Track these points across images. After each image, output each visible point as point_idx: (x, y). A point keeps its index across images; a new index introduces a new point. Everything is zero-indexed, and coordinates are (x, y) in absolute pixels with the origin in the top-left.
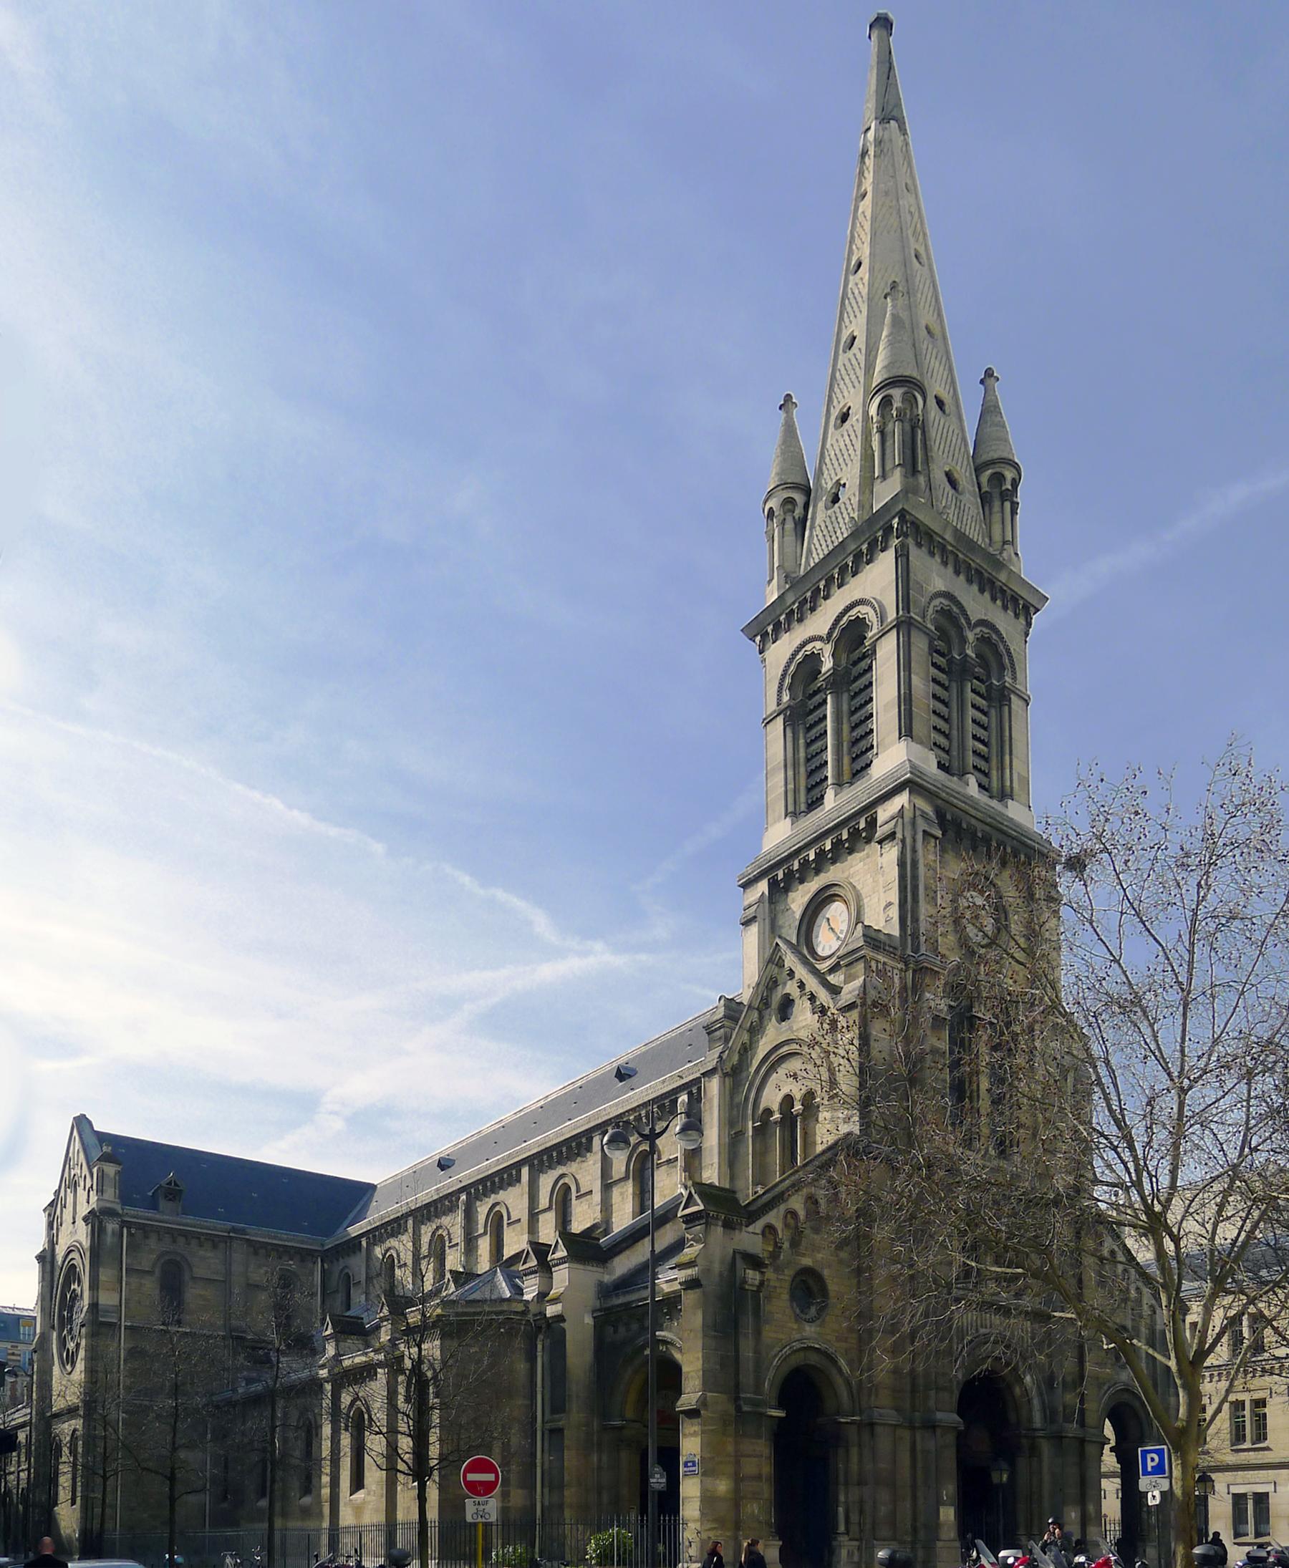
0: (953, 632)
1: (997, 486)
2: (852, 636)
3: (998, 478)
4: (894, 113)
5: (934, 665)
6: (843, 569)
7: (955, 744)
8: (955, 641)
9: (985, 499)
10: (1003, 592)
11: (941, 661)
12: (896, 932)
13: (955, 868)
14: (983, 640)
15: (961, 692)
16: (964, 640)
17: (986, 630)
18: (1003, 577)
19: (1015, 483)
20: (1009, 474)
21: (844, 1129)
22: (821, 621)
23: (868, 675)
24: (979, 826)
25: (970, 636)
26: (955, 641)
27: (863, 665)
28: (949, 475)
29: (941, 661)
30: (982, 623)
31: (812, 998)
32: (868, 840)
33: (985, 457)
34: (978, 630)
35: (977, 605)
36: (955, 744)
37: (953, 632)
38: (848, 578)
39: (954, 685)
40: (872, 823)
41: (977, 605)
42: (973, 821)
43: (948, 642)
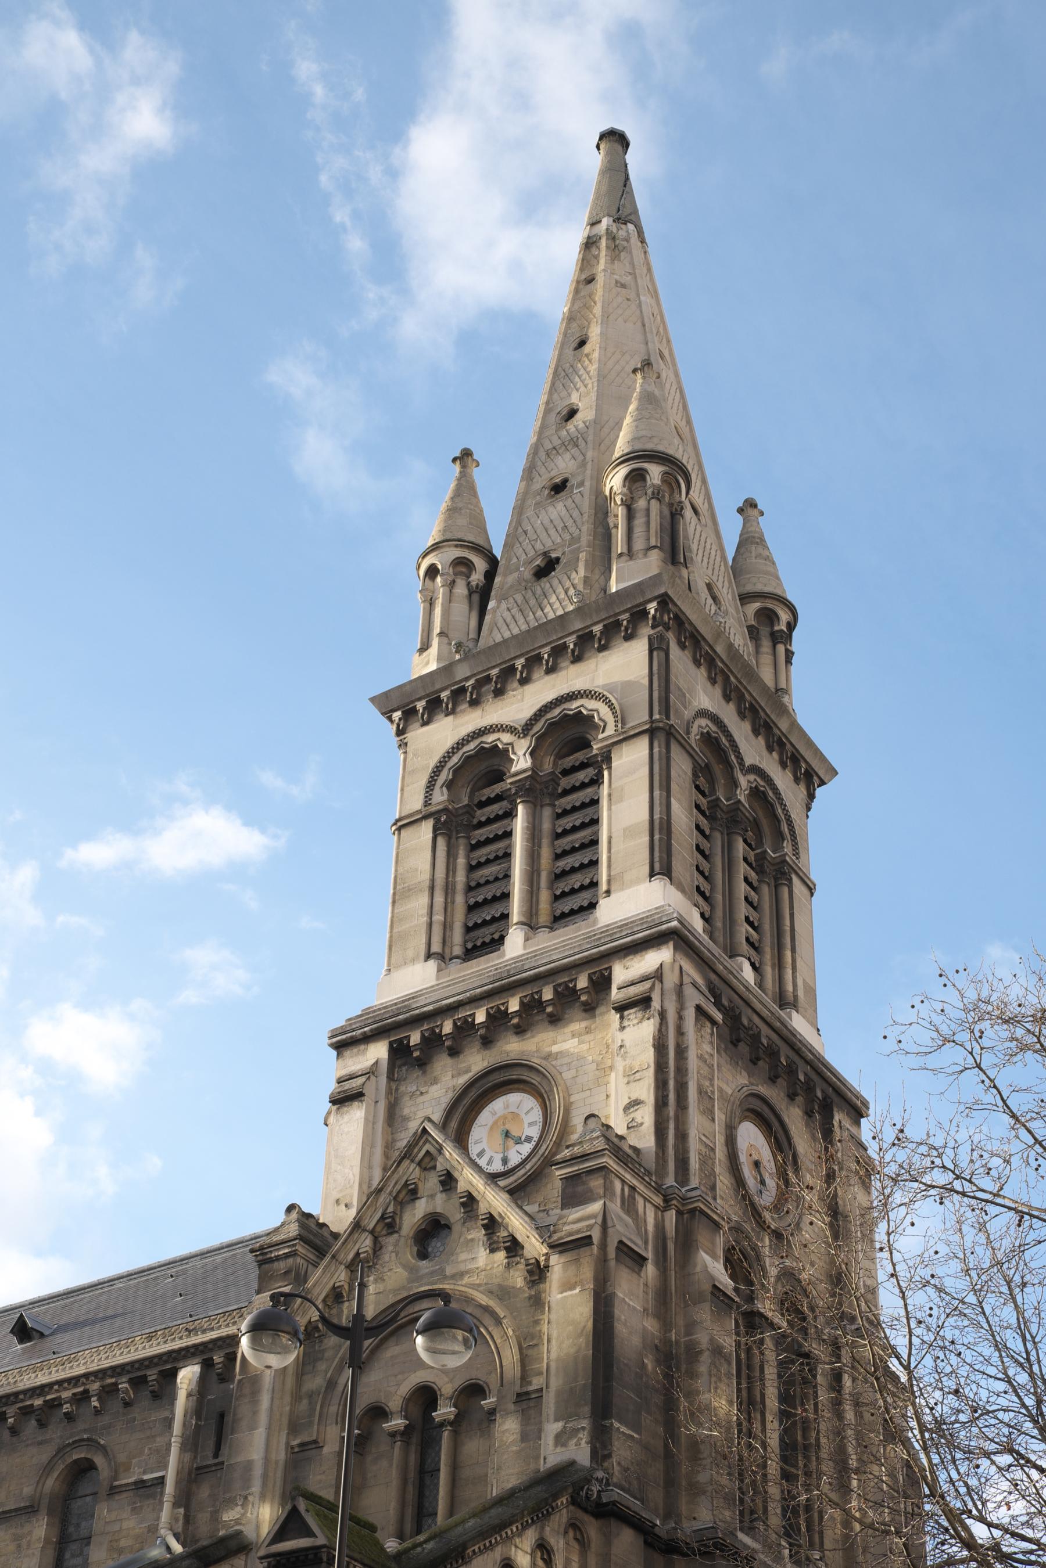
0: (717, 769)
1: (773, 622)
2: (568, 736)
3: (768, 616)
4: (632, 217)
5: (697, 787)
6: (559, 651)
7: (719, 912)
8: (721, 781)
9: (753, 633)
10: (781, 744)
11: (703, 802)
12: (645, 1139)
13: (732, 1081)
14: (756, 793)
15: (728, 849)
16: (735, 784)
17: (762, 783)
18: (783, 725)
19: (791, 626)
20: (784, 616)
21: (552, 1456)
22: (520, 704)
23: (589, 790)
24: (765, 1030)
25: (743, 781)
26: (721, 781)
27: (582, 776)
28: (709, 586)
29: (703, 802)
30: (755, 770)
31: (492, 1224)
32: (589, 1009)
33: (749, 588)
34: (752, 777)
35: (752, 750)
36: (719, 912)
37: (717, 769)
38: (564, 663)
39: (717, 836)
40: (602, 983)
41: (752, 750)
42: (756, 1020)
43: (712, 781)
